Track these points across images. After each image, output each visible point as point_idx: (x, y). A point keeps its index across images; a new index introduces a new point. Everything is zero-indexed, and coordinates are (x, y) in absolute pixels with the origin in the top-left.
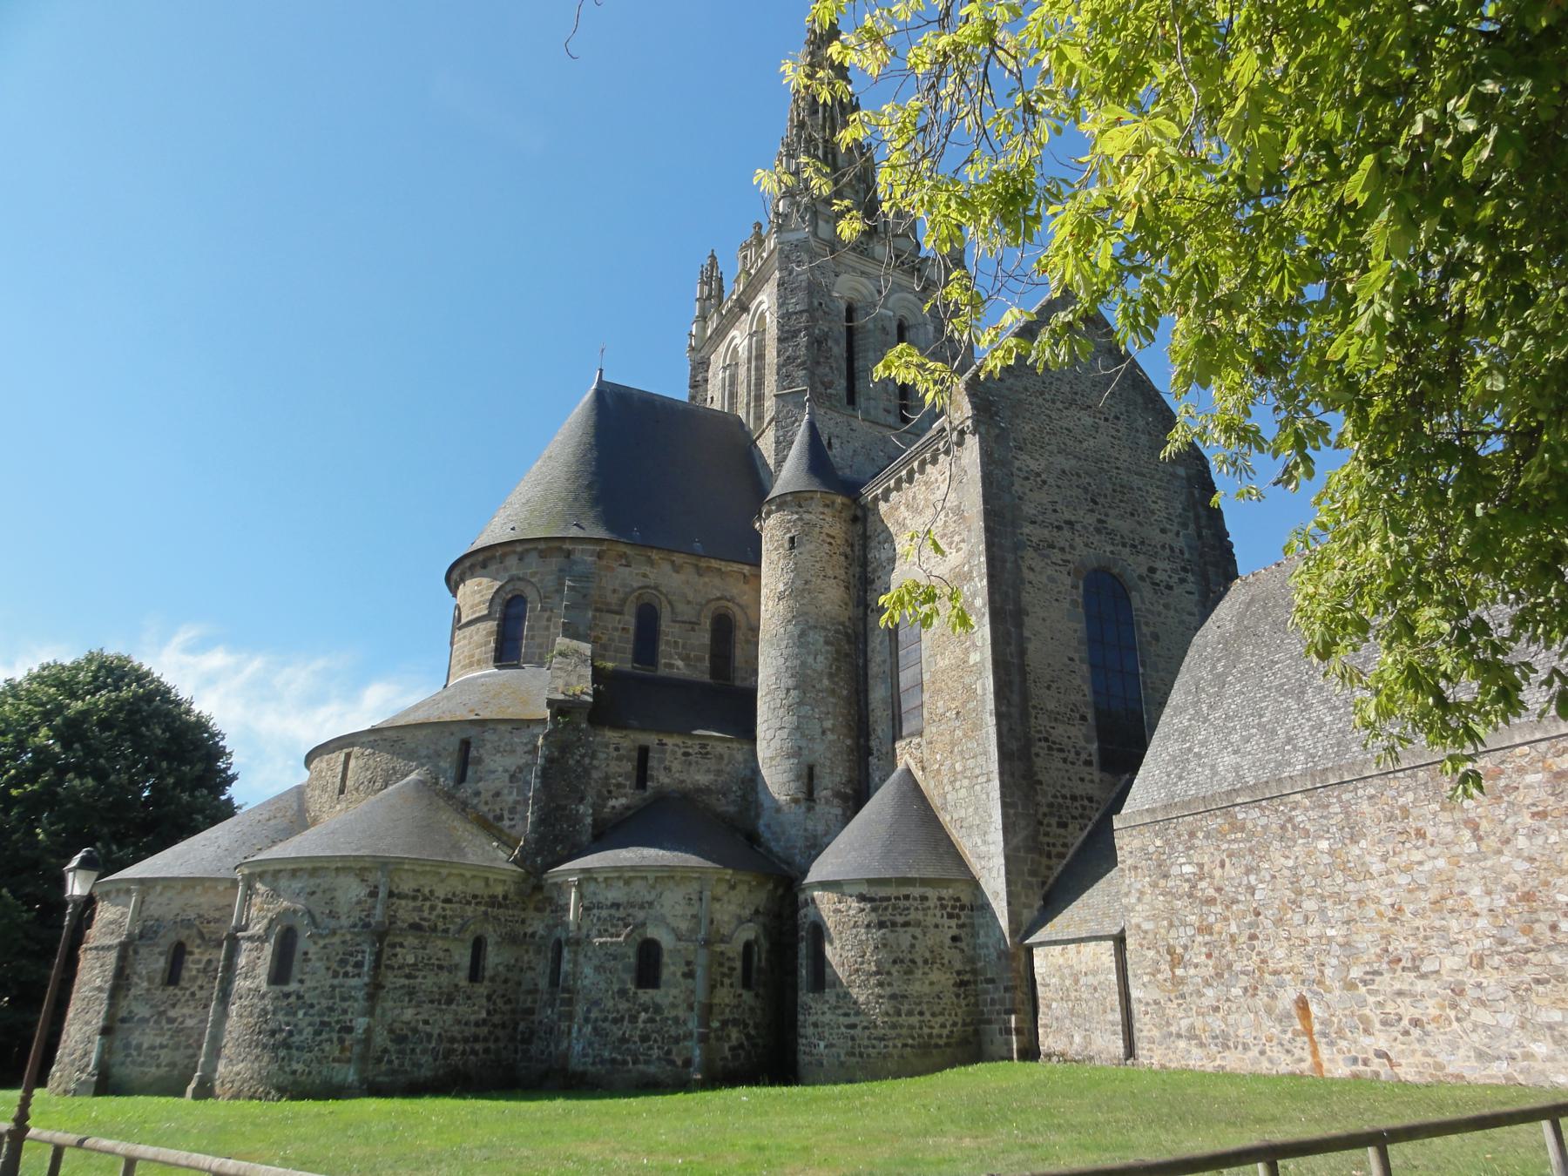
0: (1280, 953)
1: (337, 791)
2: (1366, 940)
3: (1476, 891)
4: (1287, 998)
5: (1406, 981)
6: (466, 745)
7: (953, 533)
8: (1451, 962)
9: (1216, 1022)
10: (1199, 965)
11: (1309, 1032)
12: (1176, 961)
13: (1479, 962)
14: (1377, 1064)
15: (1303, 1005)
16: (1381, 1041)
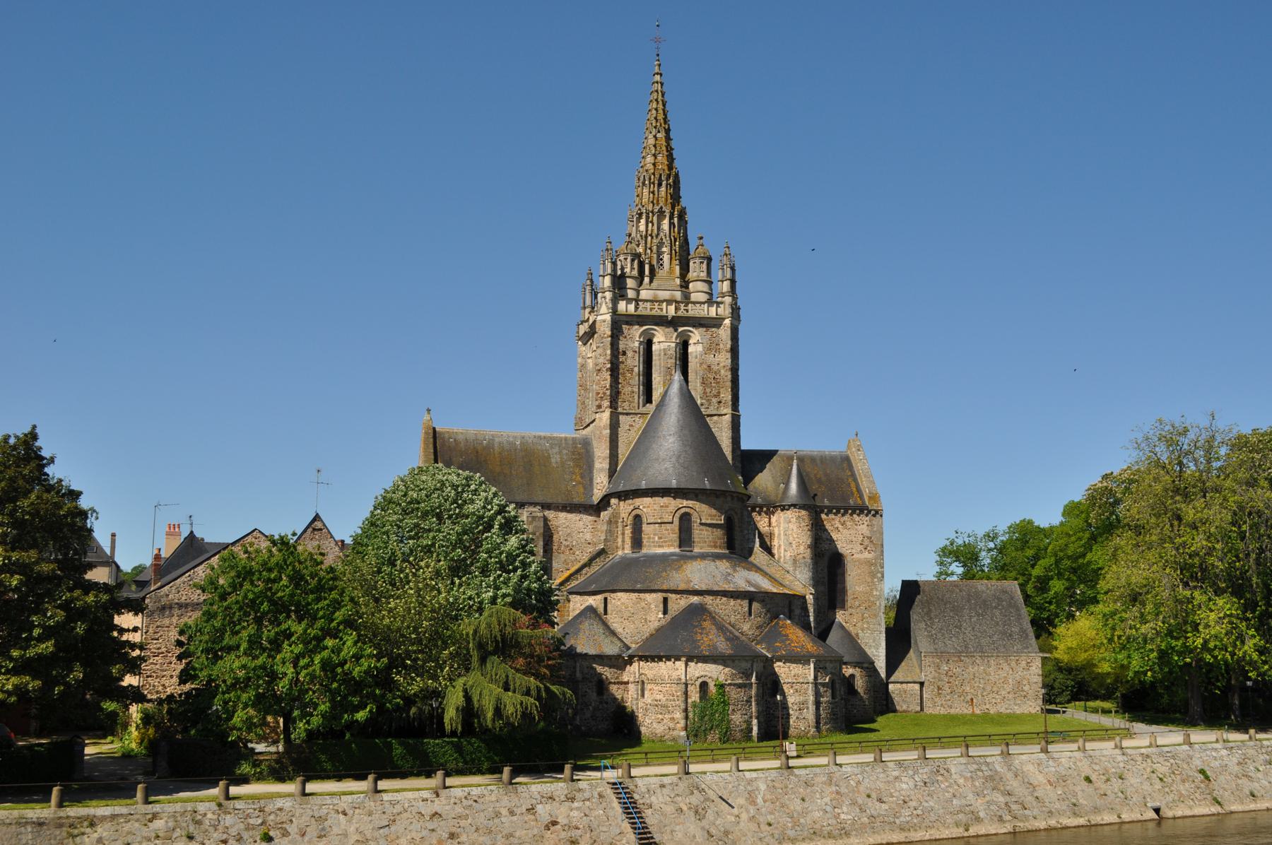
0: (968, 689)
1: (747, 614)
2: (989, 688)
3: (1010, 680)
4: (968, 698)
5: (995, 695)
6: (790, 602)
7: (867, 546)
8: (1003, 693)
9: (949, 703)
10: (947, 689)
11: (972, 705)
12: (939, 688)
13: (1009, 693)
14: (986, 711)
15: (972, 699)
16: (988, 707)
